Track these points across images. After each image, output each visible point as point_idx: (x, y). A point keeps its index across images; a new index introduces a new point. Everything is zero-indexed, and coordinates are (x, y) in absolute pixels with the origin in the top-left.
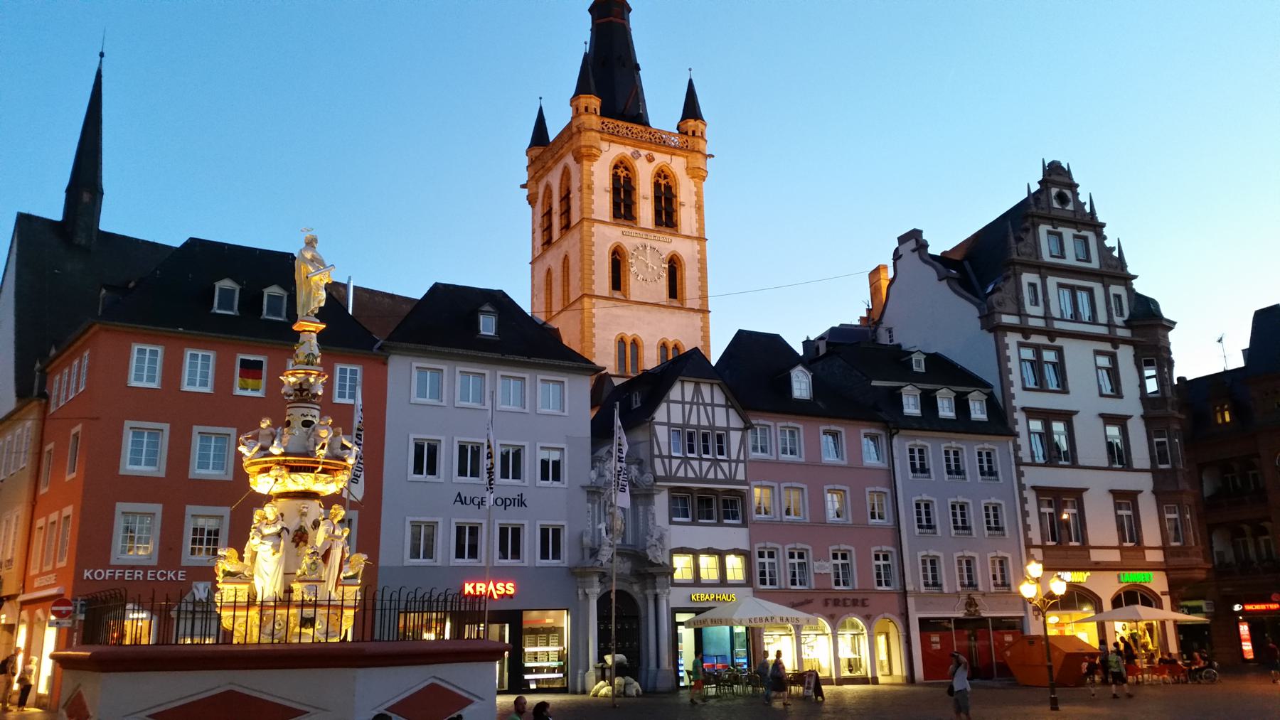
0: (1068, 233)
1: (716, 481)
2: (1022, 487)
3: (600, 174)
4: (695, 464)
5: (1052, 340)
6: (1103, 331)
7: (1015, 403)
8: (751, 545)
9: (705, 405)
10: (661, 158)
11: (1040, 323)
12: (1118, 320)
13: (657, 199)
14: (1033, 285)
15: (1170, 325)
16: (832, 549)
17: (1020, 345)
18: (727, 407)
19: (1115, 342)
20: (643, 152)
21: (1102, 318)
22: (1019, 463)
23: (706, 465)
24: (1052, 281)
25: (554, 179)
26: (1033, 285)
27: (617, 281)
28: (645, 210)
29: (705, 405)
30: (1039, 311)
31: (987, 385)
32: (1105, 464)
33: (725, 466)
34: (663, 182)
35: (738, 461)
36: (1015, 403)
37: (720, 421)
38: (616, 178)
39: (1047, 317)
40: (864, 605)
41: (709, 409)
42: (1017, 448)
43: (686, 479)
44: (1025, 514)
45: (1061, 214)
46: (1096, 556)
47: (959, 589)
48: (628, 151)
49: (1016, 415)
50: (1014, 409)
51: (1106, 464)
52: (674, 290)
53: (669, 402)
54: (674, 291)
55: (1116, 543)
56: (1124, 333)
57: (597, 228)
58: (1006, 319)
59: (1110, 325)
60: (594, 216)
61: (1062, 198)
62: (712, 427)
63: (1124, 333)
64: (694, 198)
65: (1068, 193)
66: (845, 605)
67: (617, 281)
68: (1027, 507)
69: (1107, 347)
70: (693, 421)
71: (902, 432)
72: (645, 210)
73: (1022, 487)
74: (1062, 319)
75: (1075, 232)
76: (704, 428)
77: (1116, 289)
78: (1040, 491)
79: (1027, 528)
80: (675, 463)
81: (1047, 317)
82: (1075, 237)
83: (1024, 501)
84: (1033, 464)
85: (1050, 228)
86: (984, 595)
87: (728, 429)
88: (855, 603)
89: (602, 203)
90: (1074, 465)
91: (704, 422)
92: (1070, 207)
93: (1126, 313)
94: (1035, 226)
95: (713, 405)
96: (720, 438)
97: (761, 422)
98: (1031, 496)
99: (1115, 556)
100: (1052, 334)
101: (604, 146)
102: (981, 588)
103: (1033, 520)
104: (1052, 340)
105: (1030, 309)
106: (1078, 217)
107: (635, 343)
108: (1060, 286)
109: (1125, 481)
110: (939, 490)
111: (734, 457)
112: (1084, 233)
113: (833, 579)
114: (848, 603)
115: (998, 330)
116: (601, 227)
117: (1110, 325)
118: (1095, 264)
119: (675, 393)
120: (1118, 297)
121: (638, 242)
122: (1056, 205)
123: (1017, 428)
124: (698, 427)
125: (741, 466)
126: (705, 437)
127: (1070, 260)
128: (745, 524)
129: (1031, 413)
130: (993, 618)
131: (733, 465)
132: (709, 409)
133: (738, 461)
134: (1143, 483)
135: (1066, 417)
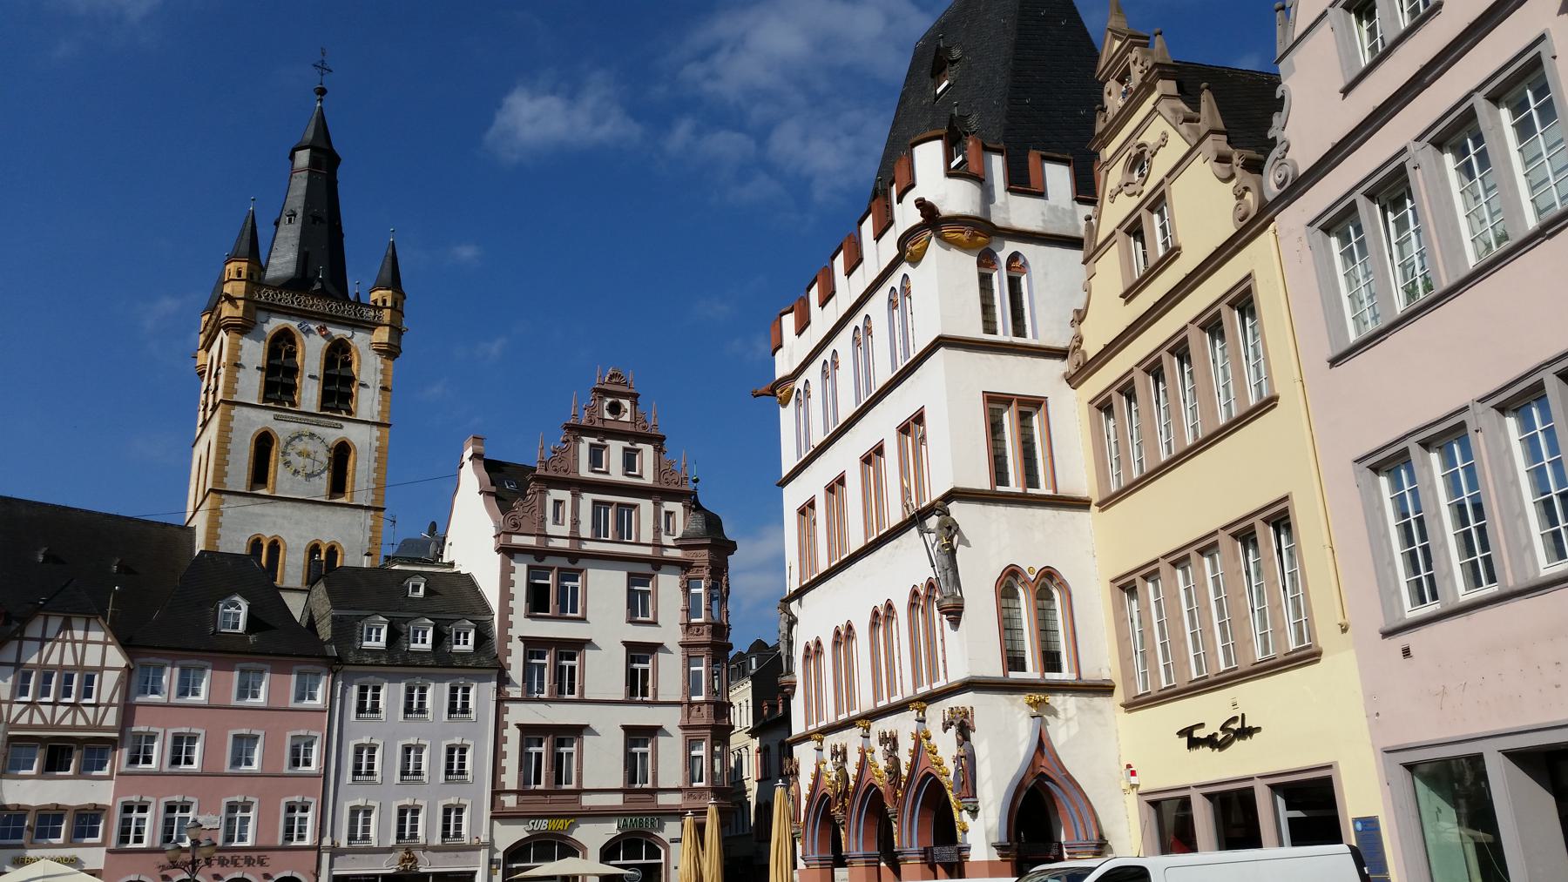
0: (616, 448)
1: (74, 727)
2: (499, 725)
3: (254, 352)
4: (47, 710)
5: (574, 562)
6: (648, 551)
7: (510, 632)
8: (115, 800)
9: (74, 642)
10: (337, 332)
11: (565, 544)
12: (667, 540)
13: (328, 380)
14: (558, 503)
15: (731, 547)
16: (225, 801)
17: (529, 568)
18: (105, 644)
19: (658, 564)
20: (313, 327)
21: (647, 535)
22: (502, 700)
23: (61, 710)
24: (587, 499)
25: (215, 349)
26: (558, 503)
27: (260, 473)
28: (309, 394)
29: (74, 642)
30: (565, 530)
31: (489, 611)
32: (621, 694)
33: (90, 711)
34: (340, 358)
35: (110, 704)
36: (510, 632)
37: (92, 658)
38: (273, 352)
39: (575, 537)
40: (262, 863)
41: (79, 646)
42: (503, 680)
43: (30, 726)
44: (498, 754)
45: (608, 426)
46: (588, 801)
47: (393, 841)
48: (294, 325)
49: (509, 646)
50: (510, 639)
51: (622, 697)
52: (338, 484)
53: (22, 639)
54: (338, 484)
55: (620, 785)
56: (677, 553)
57: (237, 412)
58: (517, 540)
59: (658, 545)
60: (236, 398)
61: (615, 409)
62: (80, 667)
63: (678, 553)
64: (380, 377)
65: (626, 404)
66: (236, 864)
67: (260, 473)
68: (505, 747)
69: (645, 569)
70: (54, 660)
71: (346, 668)
72: (309, 394)
73: (499, 725)
74: (595, 538)
75: (627, 444)
76: (68, 668)
77: (668, 506)
78: (525, 729)
79: (497, 770)
80: (17, 709)
81: (575, 537)
82: (625, 449)
83: (499, 740)
84: (527, 699)
85: (594, 441)
86: (425, 848)
87: (101, 669)
88: (249, 862)
89: (251, 384)
90: (582, 701)
91: (69, 661)
92: (627, 417)
93: (679, 534)
94: (577, 440)
95: (85, 642)
96: (90, 680)
97: (152, 660)
98: (513, 735)
99: (617, 800)
100: (574, 556)
101: (261, 316)
102: (422, 841)
103: (511, 763)
104: (574, 562)
105: (551, 529)
106: (639, 430)
107: (275, 547)
108: (595, 502)
109: (640, 716)
110: (435, 729)
111: (104, 699)
112: (639, 446)
113: (221, 833)
114: (241, 862)
115: (507, 551)
116: (245, 410)
117: (658, 545)
118: (648, 479)
119: (34, 630)
120: (669, 514)
121: (293, 427)
122: (607, 415)
123: (509, 660)
124: (61, 667)
125: (113, 711)
126: (69, 679)
127: (616, 474)
128: (109, 778)
129: (528, 641)
130: (434, 874)
131: (101, 709)
132: (79, 646)
133: (110, 704)
134: (670, 719)
135: (581, 645)
